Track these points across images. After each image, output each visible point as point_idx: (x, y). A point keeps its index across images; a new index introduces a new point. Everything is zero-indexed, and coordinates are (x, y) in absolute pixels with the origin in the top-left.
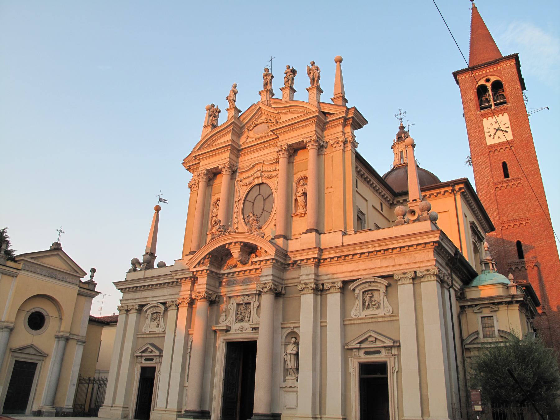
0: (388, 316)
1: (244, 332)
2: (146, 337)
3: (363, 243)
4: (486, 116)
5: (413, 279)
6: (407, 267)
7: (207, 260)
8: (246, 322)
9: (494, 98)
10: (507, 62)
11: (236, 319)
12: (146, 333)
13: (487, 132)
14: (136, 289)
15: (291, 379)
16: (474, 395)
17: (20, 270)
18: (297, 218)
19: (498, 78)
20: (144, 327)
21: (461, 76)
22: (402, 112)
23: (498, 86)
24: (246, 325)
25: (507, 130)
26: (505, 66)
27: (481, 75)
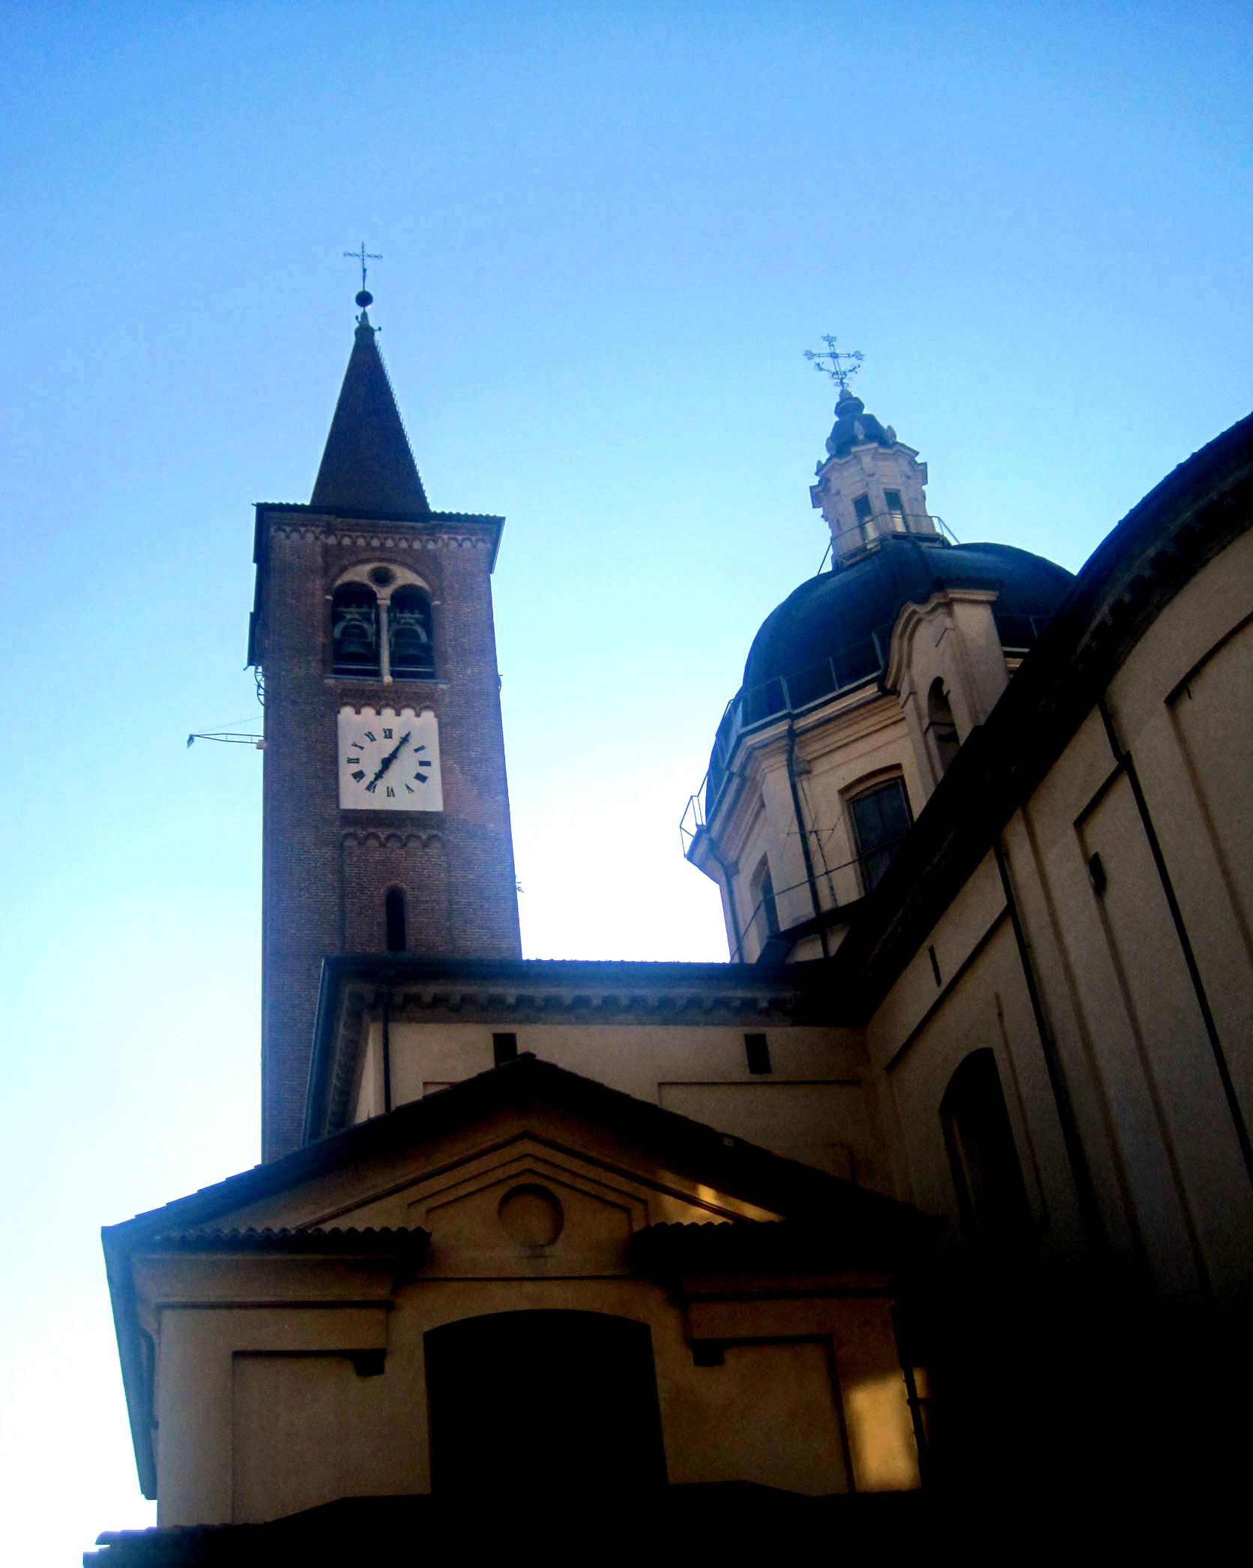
13: (350, 761)
19: (419, 582)
25: (424, 771)
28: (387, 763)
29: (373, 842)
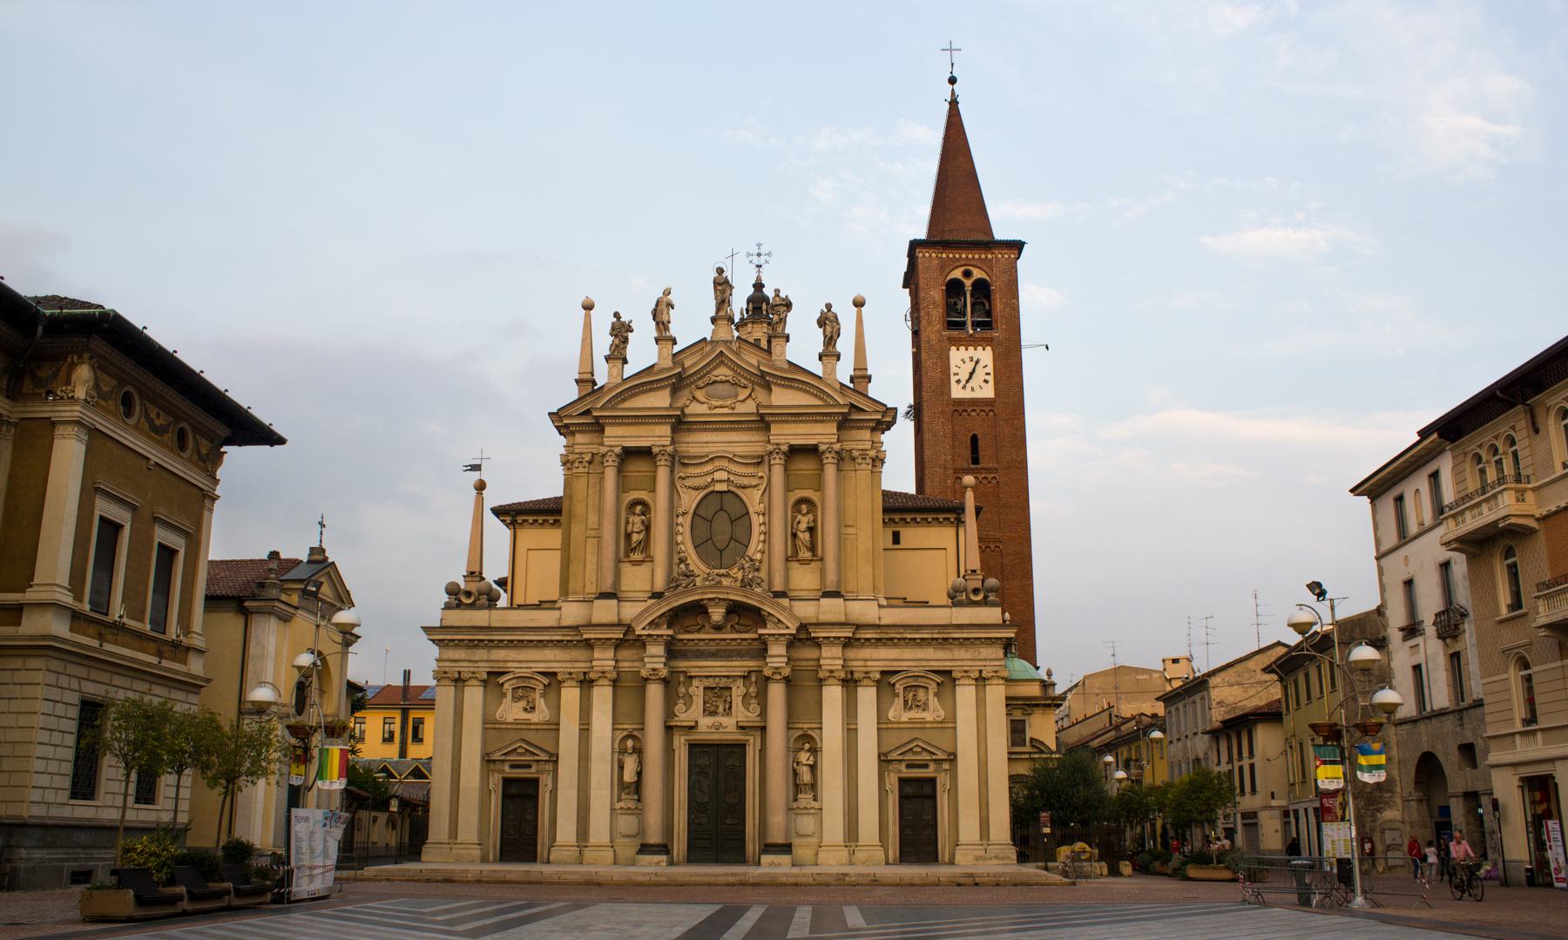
0: (938, 722)
1: (721, 730)
2: (507, 729)
3: (918, 626)
4: (957, 342)
5: (976, 679)
6: (970, 663)
7: (664, 619)
8: (723, 715)
9: (972, 313)
10: (1005, 251)
11: (704, 710)
12: (507, 721)
13: (954, 374)
14: (473, 645)
16: (1044, 817)
17: (296, 608)
18: (796, 564)
19: (984, 276)
20: (500, 711)
21: (924, 251)
22: (762, 251)
23: (982, 288)
24: (729, 722)
25: (987, 378)
26: (1000, 256)
27: (958, 260)
28: (971, 374)
29: (964, 414)
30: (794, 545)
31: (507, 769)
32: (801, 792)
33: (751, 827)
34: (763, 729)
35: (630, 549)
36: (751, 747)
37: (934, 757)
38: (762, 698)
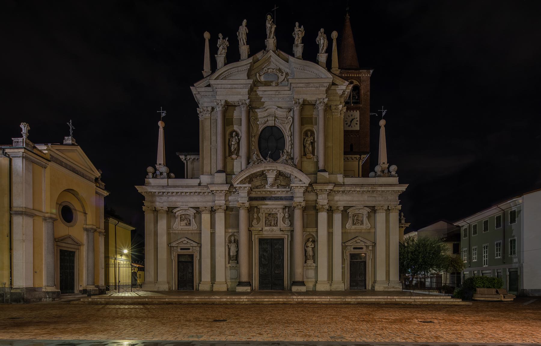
1: (273, 232)
8: (273, 226)
15: (310, 262)
20: (175, 225)
30: (304, 151)
31: (179, 250)
32: (308, 260)
33: (286, 275)
34: (292, 231)
35: (231, 153)
36: (286, 239)
37: (366, 244)
38: (291, 217)
